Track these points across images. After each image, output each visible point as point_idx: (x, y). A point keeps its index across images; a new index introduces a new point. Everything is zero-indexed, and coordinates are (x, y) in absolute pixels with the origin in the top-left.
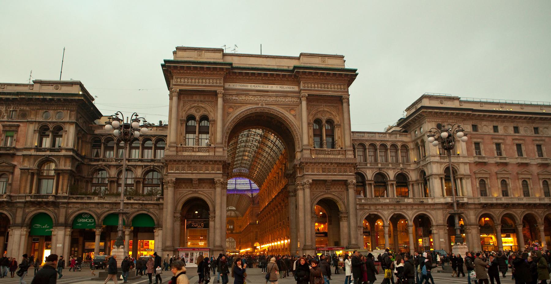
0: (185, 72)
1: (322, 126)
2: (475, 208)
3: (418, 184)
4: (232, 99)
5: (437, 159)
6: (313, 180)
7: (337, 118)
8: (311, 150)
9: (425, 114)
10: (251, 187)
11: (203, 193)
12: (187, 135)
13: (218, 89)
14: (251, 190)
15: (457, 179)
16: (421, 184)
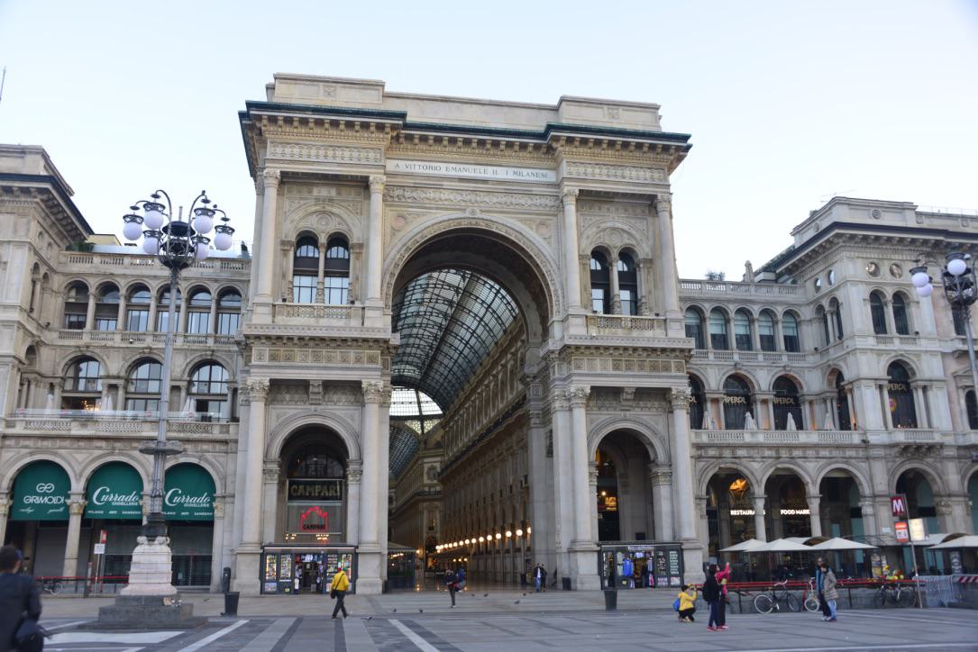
0: (295, 130)
1: (611, 264)
2: (959, 457)
3: (825, 401)
4: (404, 197)
5: (871, 342)
6: (592, 388)
7: (644, 245)
8: (586, 317)
9: (841, 241)
10: (420, 411)
11: (336, 415)
12: (297, 278)
13: (372, 173)
14: (422, 418)
15: (916, 389)
16: (832, 400)
